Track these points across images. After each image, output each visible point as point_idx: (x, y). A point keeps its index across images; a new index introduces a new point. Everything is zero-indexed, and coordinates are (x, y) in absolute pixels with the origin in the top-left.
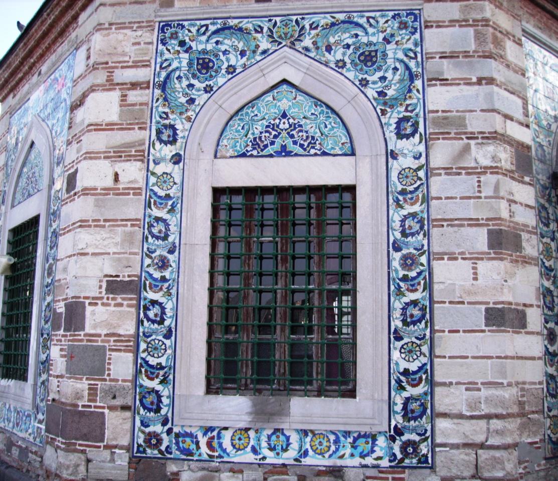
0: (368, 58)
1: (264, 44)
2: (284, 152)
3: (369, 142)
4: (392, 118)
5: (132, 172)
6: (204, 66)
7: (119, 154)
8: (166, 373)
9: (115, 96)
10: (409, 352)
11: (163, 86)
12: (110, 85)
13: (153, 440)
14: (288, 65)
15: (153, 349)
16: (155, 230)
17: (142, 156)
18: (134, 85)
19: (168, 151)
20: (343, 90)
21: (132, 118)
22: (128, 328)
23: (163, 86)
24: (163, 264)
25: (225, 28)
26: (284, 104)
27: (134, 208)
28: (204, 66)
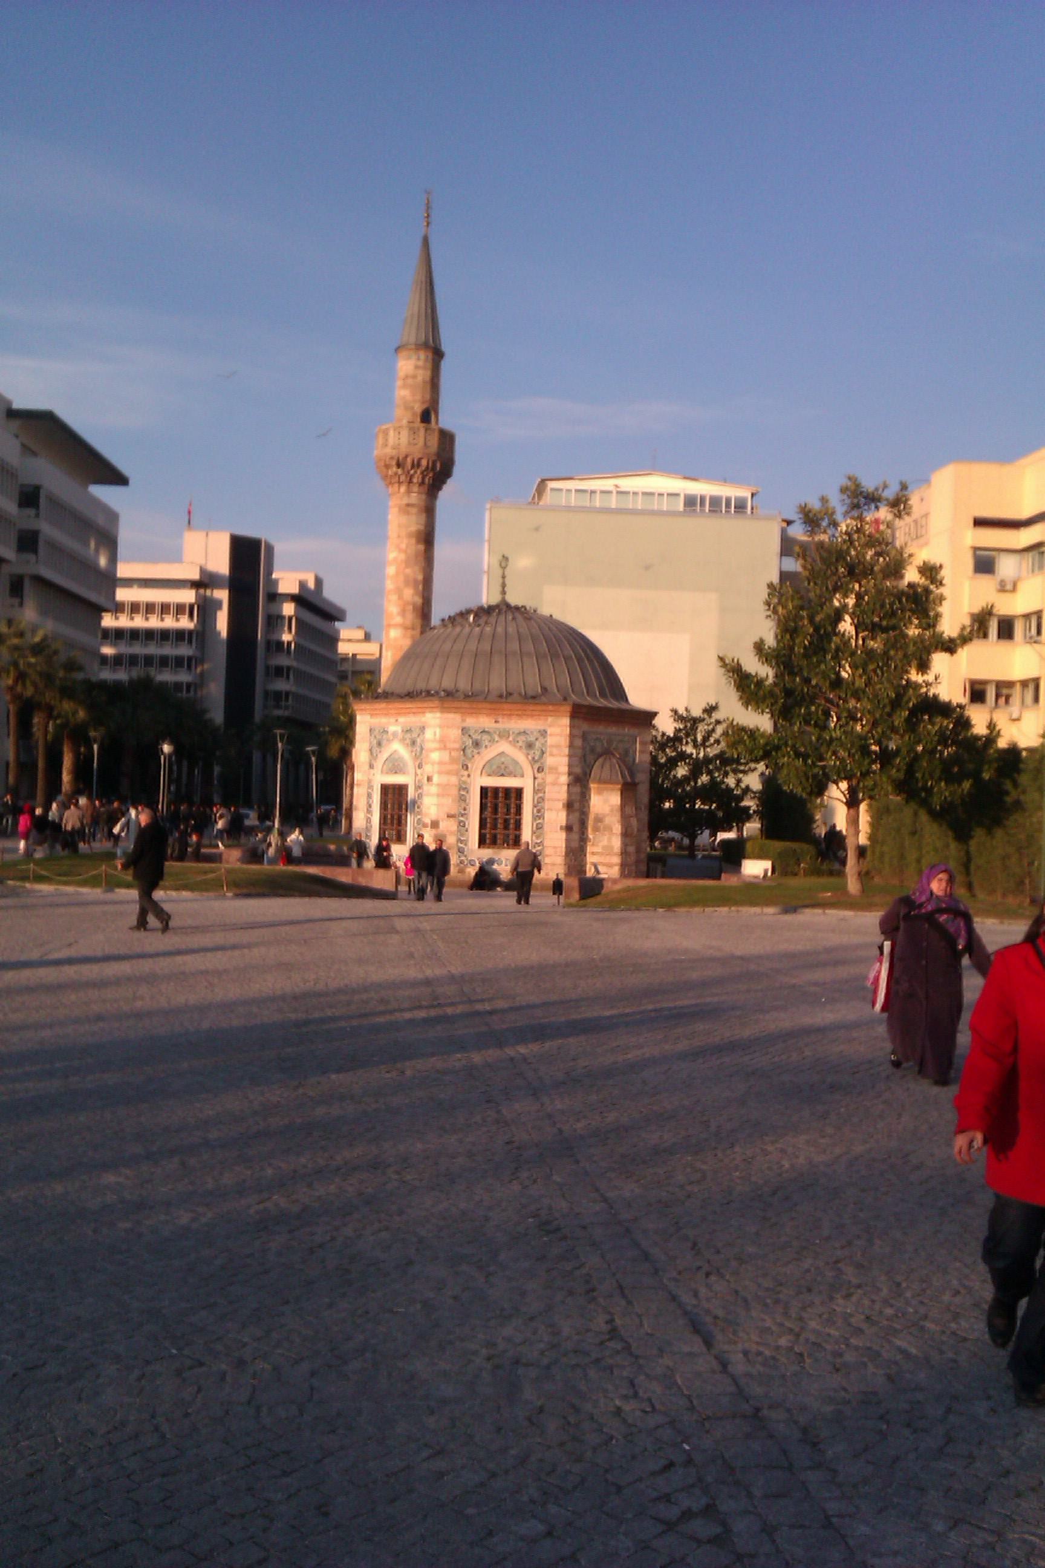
0: (530, 746)
1: (497, 738)
2: (502, 775)
3: (529, 772)
4: (536, 766)
5: (454, 780)
6: (477, 744)
7: (449, 773)
8: (465, 842)
9: (447, 753)
10: (537, 838)
11: (464, 750)
12: (445, 748)
13: (462, 862)
14: (504, 747)
15: (462, 835)
16: (462, 799)
17: (457, 774)
18: (454, 749)
19: (466, 773)
20: (520, 757)
21: (453, 761)
22: (455, 828)
23: (464, 750)
24: (465, 809)
25: (483, 732)
26: (503, 759)
27: (454, 792)
28: (477, 744)
